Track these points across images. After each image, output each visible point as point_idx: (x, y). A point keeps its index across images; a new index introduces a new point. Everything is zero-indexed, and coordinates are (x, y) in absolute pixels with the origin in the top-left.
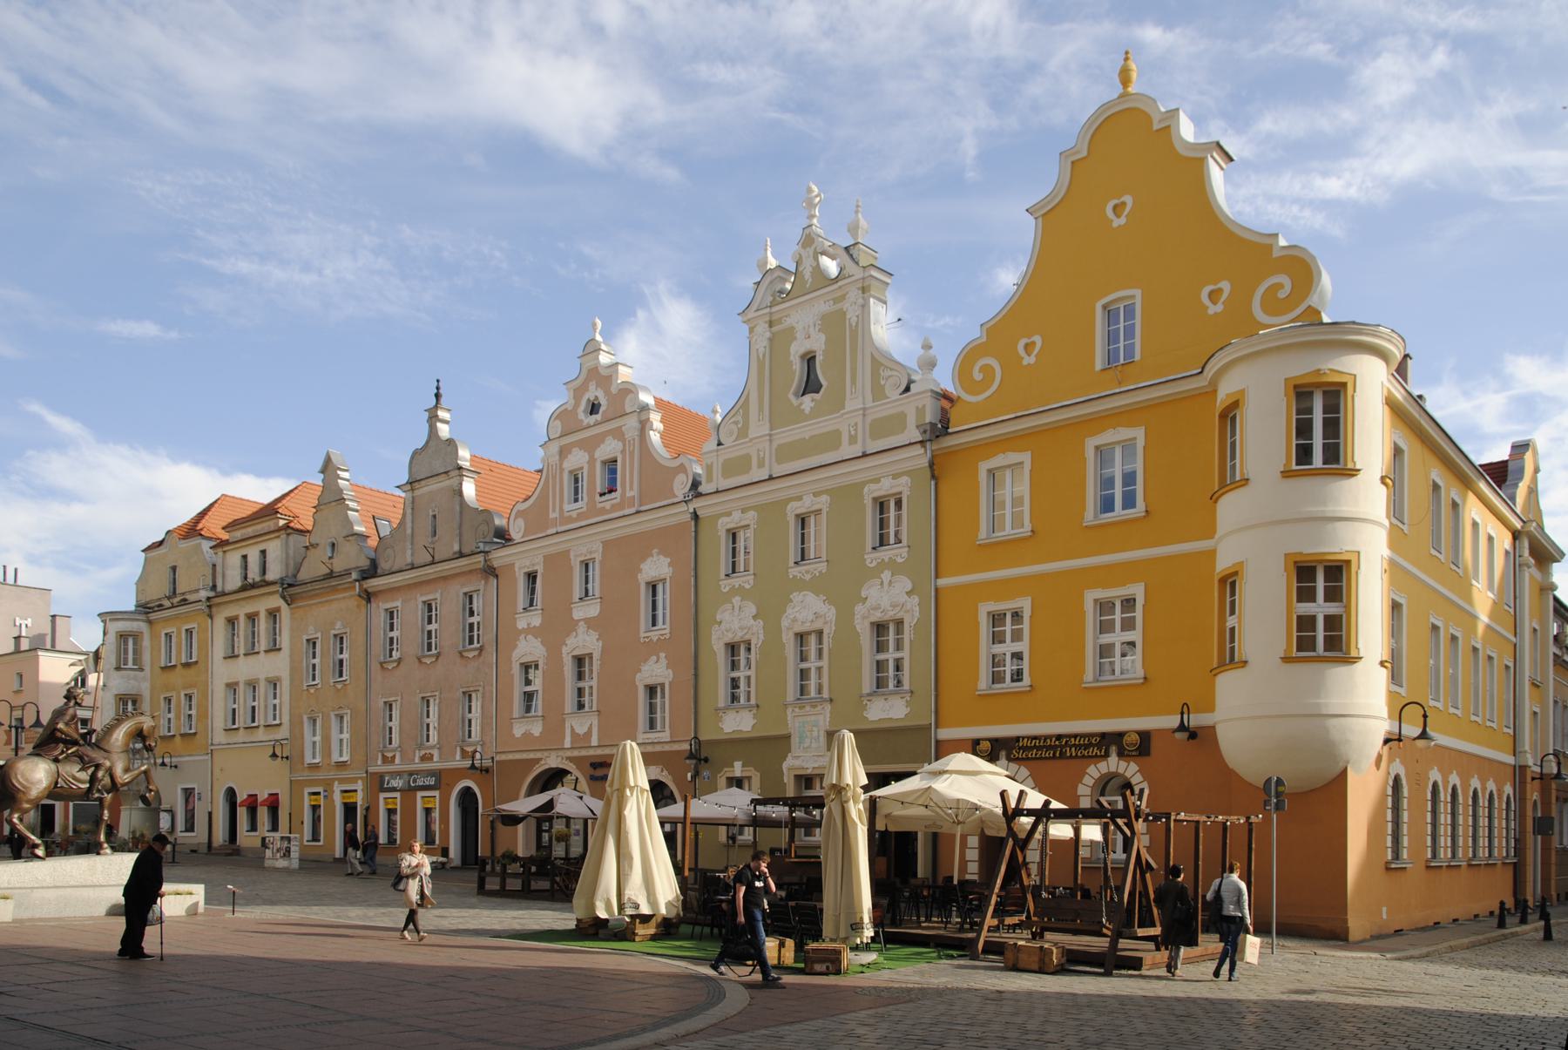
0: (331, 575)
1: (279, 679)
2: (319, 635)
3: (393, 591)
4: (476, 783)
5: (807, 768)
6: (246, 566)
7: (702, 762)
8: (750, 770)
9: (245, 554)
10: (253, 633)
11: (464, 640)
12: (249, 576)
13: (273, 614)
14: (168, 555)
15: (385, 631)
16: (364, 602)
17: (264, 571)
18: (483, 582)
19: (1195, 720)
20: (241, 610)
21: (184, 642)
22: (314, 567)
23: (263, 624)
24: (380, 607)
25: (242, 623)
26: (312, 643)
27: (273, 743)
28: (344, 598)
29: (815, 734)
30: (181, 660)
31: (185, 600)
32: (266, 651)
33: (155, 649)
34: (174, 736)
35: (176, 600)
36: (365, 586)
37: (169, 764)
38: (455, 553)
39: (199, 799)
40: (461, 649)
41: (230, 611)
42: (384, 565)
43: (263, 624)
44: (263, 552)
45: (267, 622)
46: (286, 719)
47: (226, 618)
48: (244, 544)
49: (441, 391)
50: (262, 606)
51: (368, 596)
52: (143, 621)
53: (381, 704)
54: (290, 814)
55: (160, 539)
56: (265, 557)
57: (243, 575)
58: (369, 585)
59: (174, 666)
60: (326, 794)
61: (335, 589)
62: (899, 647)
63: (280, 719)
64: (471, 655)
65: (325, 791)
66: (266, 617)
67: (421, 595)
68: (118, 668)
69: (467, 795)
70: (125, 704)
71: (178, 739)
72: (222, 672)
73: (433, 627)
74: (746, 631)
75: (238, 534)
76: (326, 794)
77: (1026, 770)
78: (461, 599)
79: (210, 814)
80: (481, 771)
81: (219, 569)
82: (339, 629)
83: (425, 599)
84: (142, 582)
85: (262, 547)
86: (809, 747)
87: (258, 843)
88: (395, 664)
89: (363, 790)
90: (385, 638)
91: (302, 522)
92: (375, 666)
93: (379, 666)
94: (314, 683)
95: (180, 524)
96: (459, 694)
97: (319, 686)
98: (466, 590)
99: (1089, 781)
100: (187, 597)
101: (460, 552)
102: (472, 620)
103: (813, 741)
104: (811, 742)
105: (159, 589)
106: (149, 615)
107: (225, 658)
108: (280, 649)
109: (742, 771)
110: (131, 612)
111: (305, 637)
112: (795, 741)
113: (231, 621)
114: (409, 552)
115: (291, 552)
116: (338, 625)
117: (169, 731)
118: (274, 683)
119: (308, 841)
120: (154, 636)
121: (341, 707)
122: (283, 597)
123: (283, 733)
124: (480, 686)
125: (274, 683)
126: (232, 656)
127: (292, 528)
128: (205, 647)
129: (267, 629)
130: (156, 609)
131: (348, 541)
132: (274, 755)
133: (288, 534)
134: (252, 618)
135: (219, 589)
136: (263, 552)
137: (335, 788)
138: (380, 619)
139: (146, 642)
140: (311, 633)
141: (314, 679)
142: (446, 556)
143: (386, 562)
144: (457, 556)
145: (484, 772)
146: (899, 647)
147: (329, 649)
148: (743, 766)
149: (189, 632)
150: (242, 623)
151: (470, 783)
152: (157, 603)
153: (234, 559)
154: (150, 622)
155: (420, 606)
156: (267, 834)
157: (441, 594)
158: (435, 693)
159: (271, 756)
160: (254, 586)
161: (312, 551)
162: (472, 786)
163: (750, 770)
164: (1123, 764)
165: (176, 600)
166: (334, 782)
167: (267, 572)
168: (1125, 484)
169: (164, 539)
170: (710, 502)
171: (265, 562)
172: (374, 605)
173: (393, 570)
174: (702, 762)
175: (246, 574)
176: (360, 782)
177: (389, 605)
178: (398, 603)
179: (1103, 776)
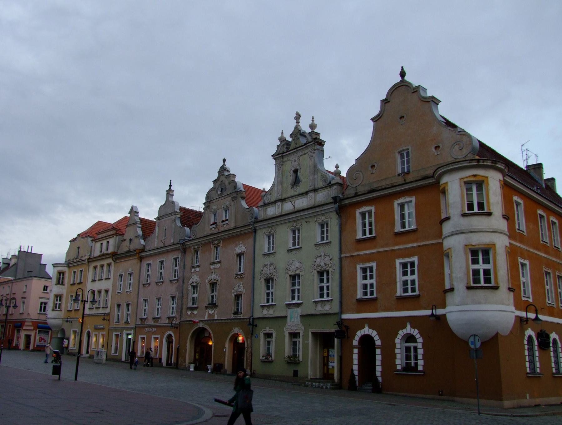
0: (129, 252)
2: (123, 273)
3: (150, 256)
4: (173, 333)
5: (293, 330)
6: (102, 247)
7: (254, 326)
8: (272, 330)
9: (102, 243)
10: (102, 272)
11: (172, 276)
12: (102, 250)
13: (109, 265)
14: (78, 244)
15: (146, 272)
16: (139, 261)
17: (107, 249)
18: (180, 254)
19: (440, 312)
20: (98, 264)
21: (79, 275)
22: (125, 247)
23: (105, 268)
24: (145, 262)
25: (99, 267)
26: (121, 276)
27: (104, 314)
28: (133, 259)
29: (296, 316)
30: (77, 281)
31: (81, 259)
32: (106, 279)
33: (70, 278)
34: (72, 310)
35: (78, 260)
36: (140, 255)
37: (69, 321)
38: (172, 243)
40: (171, 279)
41: (95, 264)
42: (147, 248)
43: (105, 268)
44: (108, 242)
45: (106, 268)
46: (109, 305)
47: (93, 266)
50: (105, 262)
51: (141, 259)
52: (66, 267)
53: (142, 300)
54: (108, 342)
55: (75, 237)
56: (108, 244)
57: (101, 251)
58: (142, 255)
60: (121, 335)
61: (130, 256)
62: (328, 281)
63: (108, 305)
64: (174, 282)
65: (120, 334)
66: (106, 266)
67: (159, 259)
69: (170, 336)
70: (57, 298)
71: (73, 311)
72: (90, 286)
73: (162, 271)
74: (272, 274)
75: (100, 236)
77: (371, 330)
78: (172, 260)
80: (175, 328)
81: (93, 248)
83: (160, 260)
84: (68, 253)
85: (108, 240)
86: (294, 321)
88: (148, 285)
89: (133, 334)
91: (122, 231)
92: (141, 285)
93: (142, 285)
94: (120, 291)
95: (83, 232)
96: (169, 297)
97: (122, 293)
98: (175, 257)
99: (399, 337)
100: (82, 258)
101: (173, 242)
102: (176, 268)
103: (296, 319)
104: (295, 319)
105: (73, 255)
108: (110, 278)
109: (269, 330)
110: (63, 264)
111: (119, 274)
112: (289, 318)
113: (95, 268)
114: (156, 243)
115: (117, 242)
116: (130, 270)
117: (71, 308)
118: (107, 291)
119: (113, 353)
120: (70, 273)
121: (128, 301)
122: (113, 260)
123: (108, 311)
124: (176, 294)
125: (107, 291)
126: (93, 281)
127: (119, 234)
128: (86, 277)
129: (106, 270)
130: (71, 263)
131: (136, 238)
132: (104, 319)
133: (117, 236)
134: (102, 266)
135: (92, 256)
136: (108, 242)
137: (124, 333)
138: (145, 268)
139: (67, 275)
140: (121, 272)
141: (120, 290)
142: (169, 244)
143: (148, 246)
144: (172, 244)
145: (176, 328)
146: (328, 281)
147: (126, 279)
148: (269, 329)
149: (81, 271)
150: (99, 267)
151: (171, 333)
153: (98, 245)
154: (69, 267)
155: (158, 262)
157: (166, 258)
158: (161, 297)
159: (103, 319)
160: (104, 255)
161: (123, 243)
162: (171, 334)
163: (272, 330)
164: (412, 330)
165: (78, 260)
166: (123, 330)
167: (109, 250)
169: (77, 237)
170: (265, 223)
171: (108, 246)
172: (142, 262)
173: (150, 249)
174: (254, 326)
175: (102, 250)
176: (133, 331)
177: (148, 262)
178: (151, 262)
179: (405, 335)
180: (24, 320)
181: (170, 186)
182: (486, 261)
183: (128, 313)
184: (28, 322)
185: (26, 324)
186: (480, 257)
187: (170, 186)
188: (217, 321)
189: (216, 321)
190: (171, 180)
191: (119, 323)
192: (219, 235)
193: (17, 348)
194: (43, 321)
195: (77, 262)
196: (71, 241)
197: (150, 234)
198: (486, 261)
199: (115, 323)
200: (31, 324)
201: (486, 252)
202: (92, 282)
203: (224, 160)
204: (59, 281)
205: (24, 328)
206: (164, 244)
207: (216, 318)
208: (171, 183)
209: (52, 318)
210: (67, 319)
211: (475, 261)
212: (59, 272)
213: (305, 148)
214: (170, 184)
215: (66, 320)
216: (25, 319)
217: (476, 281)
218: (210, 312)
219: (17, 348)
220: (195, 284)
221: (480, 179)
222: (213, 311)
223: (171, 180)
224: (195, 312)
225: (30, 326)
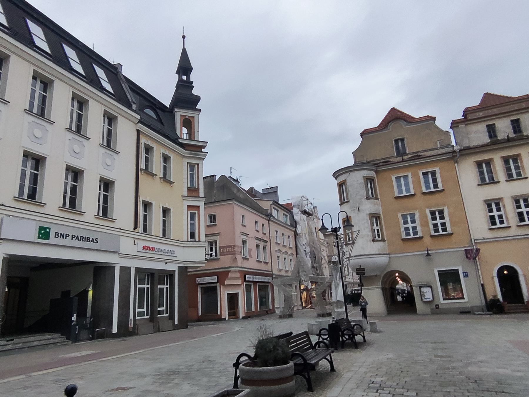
48: (478, 120)
59: (413, 195)
68: (368, 198)
79: (483, 285)
106: (378, 167)
107: (479, 185)
152: (382, 161)
154: (376, 172)
165: (405, 157)
180: (229, 269)
184: (235, 272)
185: (230, 275)
193: (220, 319)
194: (255, 271)
195: (403, 161)
196: (362, 134)
200: (238, 275)
205: (227, 282)
209: (373, 255)
210: (428, 251)
215: (427, 252)
216: (230, 267)
219: (220, 319)
225: (237, 278)
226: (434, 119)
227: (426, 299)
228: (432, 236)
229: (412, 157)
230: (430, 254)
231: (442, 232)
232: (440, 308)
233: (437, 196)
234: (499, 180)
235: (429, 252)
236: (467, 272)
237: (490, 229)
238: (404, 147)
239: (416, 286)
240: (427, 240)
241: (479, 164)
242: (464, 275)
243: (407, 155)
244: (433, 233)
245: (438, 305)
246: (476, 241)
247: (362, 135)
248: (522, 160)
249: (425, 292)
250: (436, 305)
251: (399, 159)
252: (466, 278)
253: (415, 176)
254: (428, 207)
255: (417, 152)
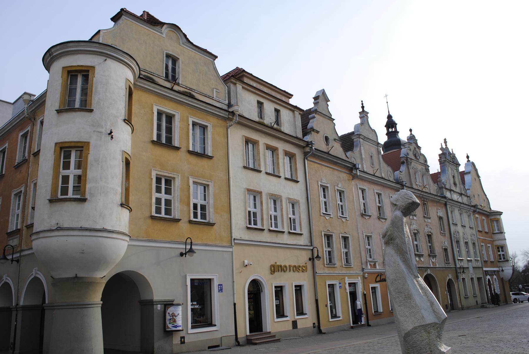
1: (298, 202)
2: (328, 185)
39: (221, 290)
49: (364, 105)
60: (341, 285)
65: (340, 283)
76: (341, 285)
79: (235, 304)
82: (340, 187)
87: (290, 327)
90: (345, 201)
156: (297, 317)
165: (176, 88)
168: (166, 205)
181: (363, 107)
182: (503, 251)
183: (329, 249)
186: (500, 249)
187: (363, 107)
188: (438, 269)
189: (437, 268)
190: (362, 101)
191: (336, 266)
192: (432, 196)
195: (172, 89)
197: (352, 148)
198: (503, 251)
199: (344, 266)
201: (502, 247)
202: (244, 170)
203: (411, 130)
204: (71, 102)
206: (374, 174)
207: (437, 266)
208: (362, 104)
211: (499, 251)
212: (69, 72)
213: (455, 165)
214: (362, 105)
217: (500, 259)
218: (433, 261)
220: (416, 232)
221: (497, 219)
222: (434, 259)
223: (362, 101)
224: (422, 259)
226: (216, 57)
227: (176, 327)
228: (190, 222)
229: (183, 91)
230: (195, 250)
231: (201, 219)
232: (186, 341)
233: (205, 162)
234: (261, 170)
235: (193, 247)
236: (222, 285)
237: (248, 228)
238: (174, 70)
239: (159, 302)
240: (184, 226)
241: (247, 141)
242: (219, 288)
243: (178, 84)
244: (192, 218)
245: (184, 337)
246: (236, 241)
247: (123, 12)
248: (278, 154)
249: (176, 314)
250: (182, 338)
251: (168, 85)
252: (221, 293)
253: (184, 120)
254: (193, 175)
255: (191, 89)
